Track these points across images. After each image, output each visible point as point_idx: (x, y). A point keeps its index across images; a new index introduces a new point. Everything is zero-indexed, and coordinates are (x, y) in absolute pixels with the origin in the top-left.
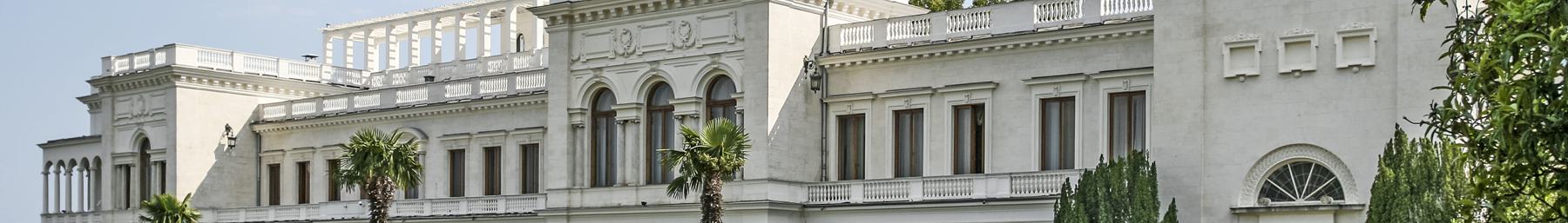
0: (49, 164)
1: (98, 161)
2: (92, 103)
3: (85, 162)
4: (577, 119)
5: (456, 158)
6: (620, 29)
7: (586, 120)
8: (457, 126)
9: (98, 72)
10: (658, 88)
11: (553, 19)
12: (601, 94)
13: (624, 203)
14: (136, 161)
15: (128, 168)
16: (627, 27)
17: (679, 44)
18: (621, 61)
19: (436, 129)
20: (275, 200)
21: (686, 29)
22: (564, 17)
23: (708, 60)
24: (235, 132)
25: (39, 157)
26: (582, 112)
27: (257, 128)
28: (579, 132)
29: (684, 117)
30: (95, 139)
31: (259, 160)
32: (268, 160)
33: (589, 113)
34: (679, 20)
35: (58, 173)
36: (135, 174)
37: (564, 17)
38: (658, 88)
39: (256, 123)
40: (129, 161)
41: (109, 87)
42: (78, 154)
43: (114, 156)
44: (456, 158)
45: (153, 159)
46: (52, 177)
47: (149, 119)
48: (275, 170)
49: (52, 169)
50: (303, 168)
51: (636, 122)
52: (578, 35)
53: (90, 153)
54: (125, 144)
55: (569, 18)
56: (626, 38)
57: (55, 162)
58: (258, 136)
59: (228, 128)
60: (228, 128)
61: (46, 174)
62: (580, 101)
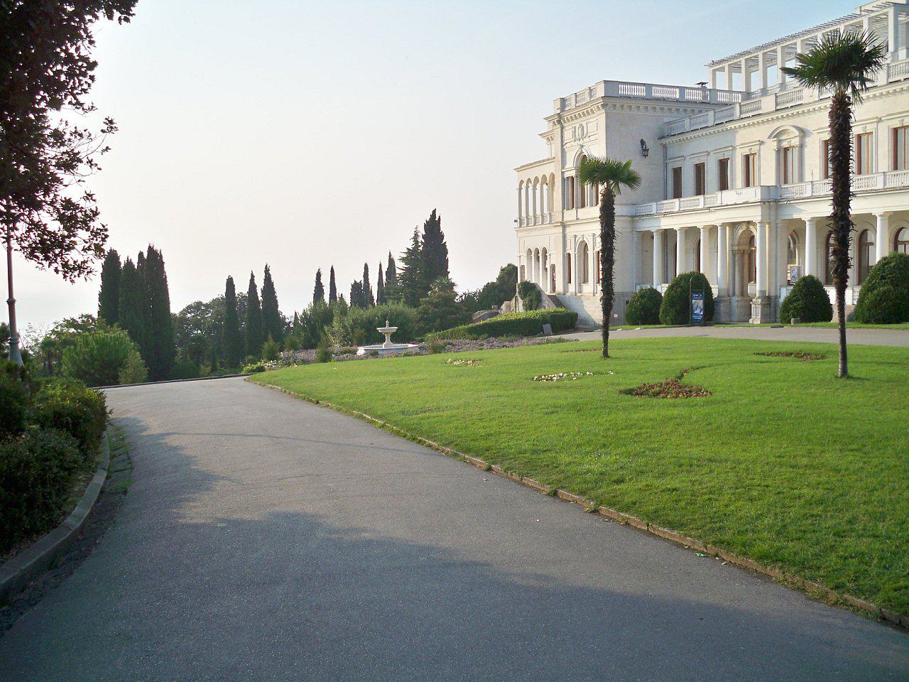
0: (522, 182)
1: (553, 176)
2: (548, 137)
3: (544, 177)
24: (649, 144)
27: (664, 141)
31: (666, 165)
32: (673, 165)
35: (527, 187)
39: (663, 137)
40: (573, 173)
41: (559, 122)
42: (538, 172)
46: (523, 191)
47: (586, 140)
48: (677, 172)
49: (524, 186)
50: (700, 169)
53: (548, 170)
57: (525, 181)
58: (665, 147)
59: (643, 142)
60: (643, 142)
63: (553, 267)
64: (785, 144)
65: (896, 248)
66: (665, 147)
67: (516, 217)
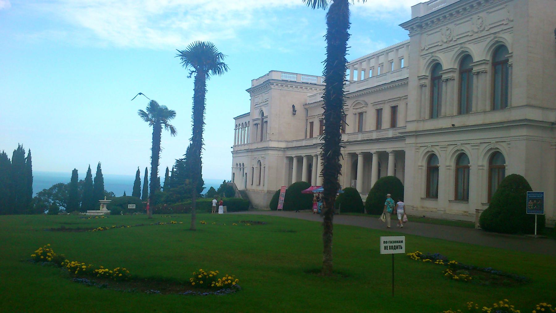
4: (423, 82)
5: (379, 112)
6: (444, 28)
7: (427, 82)
8: (380, 97)
9: (249, 86)
10: (465, 58)
11: (412, 28)
12: (436, 66)
13: (444, 126)
14: (259, 122)
15: (256, 125)
16: (449, 26)
17: (476, 30)
18: (445, 46)
19: (370, 99)
20: (311, 136)
21: (480, 20)
22: (418, 26)
23: (493, 36)
24: (296, 109)
25: (233, 123)
26: (425, 77)
28: (424, 88)
29: (478, 73)
30: (248, 114)
33: (429, 78)
34: (475, 17)
36: (259, 126)
37: (418, 26)
38: (465, 58)
43: (254, 120)
44: (379, 112)
45: (265, 120)
48: (312, 123)
51: (452, 79)
52: (425, 36)
54: (257, 115)
55: (420, 27)
56: (448, 32)
59: (293, 106)
60: (293, 106)
61: (236, 130)
62: (425, 71)
63: (246, 173)
64: (359, 111)
65: (395, 173)
66: (307, 110)
67: (232, 145)
